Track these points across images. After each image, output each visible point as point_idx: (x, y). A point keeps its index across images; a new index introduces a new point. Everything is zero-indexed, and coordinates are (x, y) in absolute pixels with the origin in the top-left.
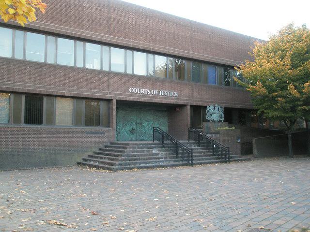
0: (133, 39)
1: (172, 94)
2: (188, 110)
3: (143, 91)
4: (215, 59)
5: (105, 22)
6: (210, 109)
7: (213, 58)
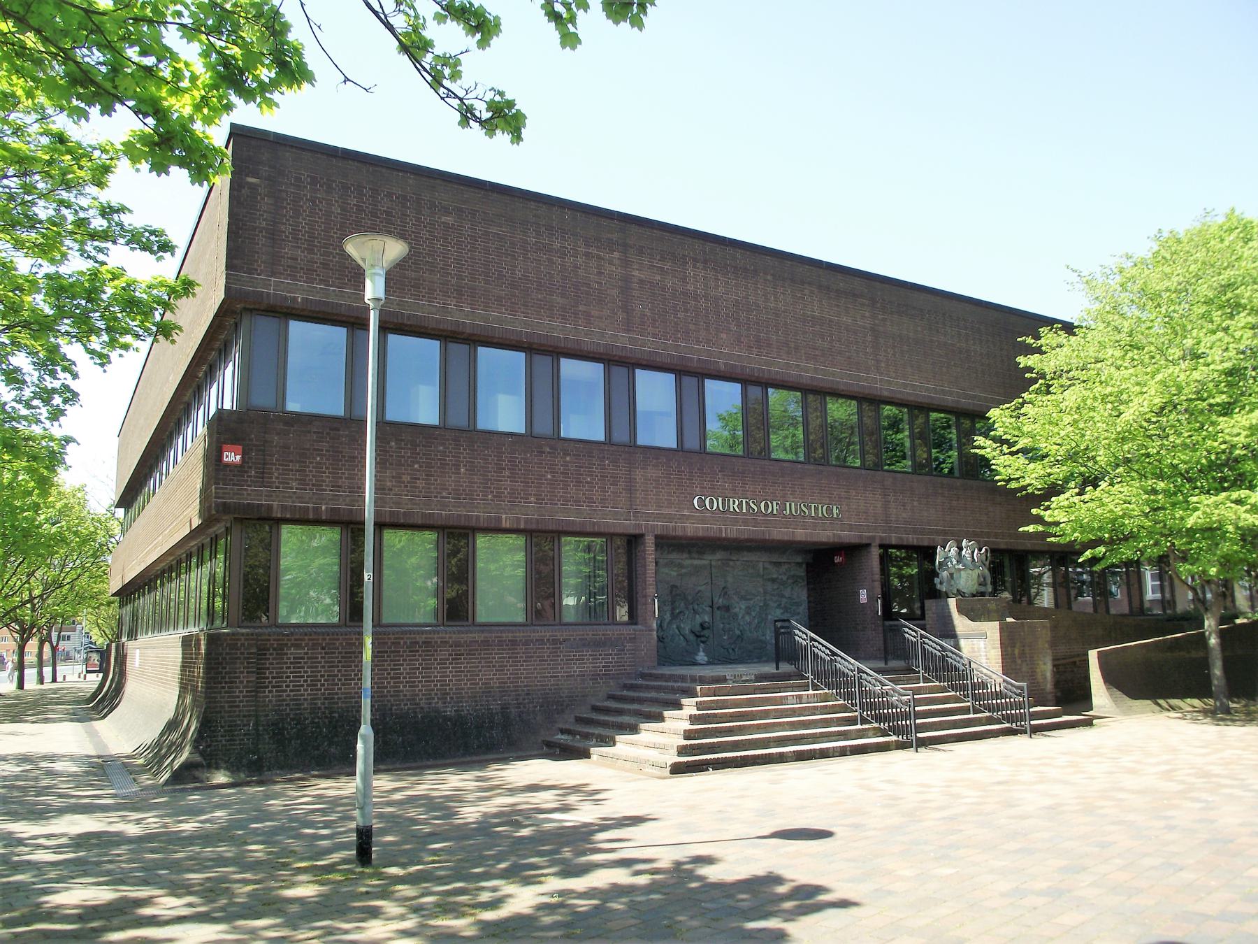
0: (698, 342)
1: (823, 510)
2: (875, 552)
3: (734, 505)
4: (951, 394)
5: (614, 292)
6: (947, 553)
7: (944, 392)
